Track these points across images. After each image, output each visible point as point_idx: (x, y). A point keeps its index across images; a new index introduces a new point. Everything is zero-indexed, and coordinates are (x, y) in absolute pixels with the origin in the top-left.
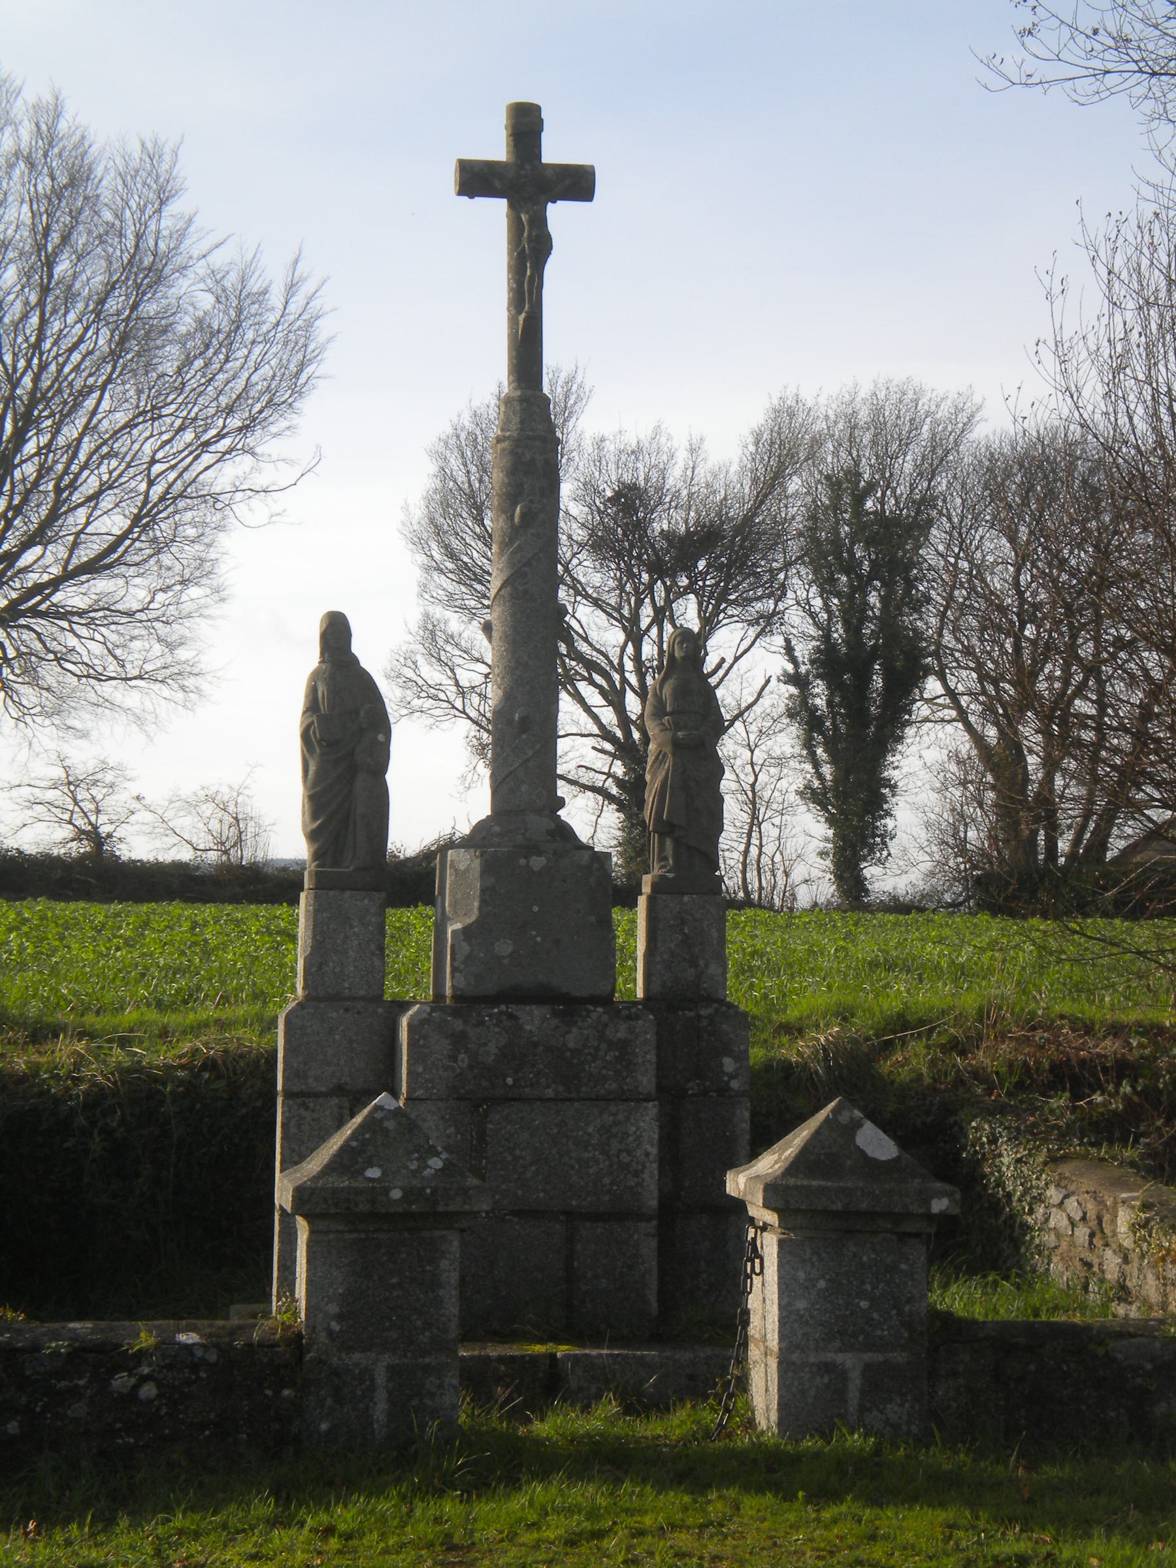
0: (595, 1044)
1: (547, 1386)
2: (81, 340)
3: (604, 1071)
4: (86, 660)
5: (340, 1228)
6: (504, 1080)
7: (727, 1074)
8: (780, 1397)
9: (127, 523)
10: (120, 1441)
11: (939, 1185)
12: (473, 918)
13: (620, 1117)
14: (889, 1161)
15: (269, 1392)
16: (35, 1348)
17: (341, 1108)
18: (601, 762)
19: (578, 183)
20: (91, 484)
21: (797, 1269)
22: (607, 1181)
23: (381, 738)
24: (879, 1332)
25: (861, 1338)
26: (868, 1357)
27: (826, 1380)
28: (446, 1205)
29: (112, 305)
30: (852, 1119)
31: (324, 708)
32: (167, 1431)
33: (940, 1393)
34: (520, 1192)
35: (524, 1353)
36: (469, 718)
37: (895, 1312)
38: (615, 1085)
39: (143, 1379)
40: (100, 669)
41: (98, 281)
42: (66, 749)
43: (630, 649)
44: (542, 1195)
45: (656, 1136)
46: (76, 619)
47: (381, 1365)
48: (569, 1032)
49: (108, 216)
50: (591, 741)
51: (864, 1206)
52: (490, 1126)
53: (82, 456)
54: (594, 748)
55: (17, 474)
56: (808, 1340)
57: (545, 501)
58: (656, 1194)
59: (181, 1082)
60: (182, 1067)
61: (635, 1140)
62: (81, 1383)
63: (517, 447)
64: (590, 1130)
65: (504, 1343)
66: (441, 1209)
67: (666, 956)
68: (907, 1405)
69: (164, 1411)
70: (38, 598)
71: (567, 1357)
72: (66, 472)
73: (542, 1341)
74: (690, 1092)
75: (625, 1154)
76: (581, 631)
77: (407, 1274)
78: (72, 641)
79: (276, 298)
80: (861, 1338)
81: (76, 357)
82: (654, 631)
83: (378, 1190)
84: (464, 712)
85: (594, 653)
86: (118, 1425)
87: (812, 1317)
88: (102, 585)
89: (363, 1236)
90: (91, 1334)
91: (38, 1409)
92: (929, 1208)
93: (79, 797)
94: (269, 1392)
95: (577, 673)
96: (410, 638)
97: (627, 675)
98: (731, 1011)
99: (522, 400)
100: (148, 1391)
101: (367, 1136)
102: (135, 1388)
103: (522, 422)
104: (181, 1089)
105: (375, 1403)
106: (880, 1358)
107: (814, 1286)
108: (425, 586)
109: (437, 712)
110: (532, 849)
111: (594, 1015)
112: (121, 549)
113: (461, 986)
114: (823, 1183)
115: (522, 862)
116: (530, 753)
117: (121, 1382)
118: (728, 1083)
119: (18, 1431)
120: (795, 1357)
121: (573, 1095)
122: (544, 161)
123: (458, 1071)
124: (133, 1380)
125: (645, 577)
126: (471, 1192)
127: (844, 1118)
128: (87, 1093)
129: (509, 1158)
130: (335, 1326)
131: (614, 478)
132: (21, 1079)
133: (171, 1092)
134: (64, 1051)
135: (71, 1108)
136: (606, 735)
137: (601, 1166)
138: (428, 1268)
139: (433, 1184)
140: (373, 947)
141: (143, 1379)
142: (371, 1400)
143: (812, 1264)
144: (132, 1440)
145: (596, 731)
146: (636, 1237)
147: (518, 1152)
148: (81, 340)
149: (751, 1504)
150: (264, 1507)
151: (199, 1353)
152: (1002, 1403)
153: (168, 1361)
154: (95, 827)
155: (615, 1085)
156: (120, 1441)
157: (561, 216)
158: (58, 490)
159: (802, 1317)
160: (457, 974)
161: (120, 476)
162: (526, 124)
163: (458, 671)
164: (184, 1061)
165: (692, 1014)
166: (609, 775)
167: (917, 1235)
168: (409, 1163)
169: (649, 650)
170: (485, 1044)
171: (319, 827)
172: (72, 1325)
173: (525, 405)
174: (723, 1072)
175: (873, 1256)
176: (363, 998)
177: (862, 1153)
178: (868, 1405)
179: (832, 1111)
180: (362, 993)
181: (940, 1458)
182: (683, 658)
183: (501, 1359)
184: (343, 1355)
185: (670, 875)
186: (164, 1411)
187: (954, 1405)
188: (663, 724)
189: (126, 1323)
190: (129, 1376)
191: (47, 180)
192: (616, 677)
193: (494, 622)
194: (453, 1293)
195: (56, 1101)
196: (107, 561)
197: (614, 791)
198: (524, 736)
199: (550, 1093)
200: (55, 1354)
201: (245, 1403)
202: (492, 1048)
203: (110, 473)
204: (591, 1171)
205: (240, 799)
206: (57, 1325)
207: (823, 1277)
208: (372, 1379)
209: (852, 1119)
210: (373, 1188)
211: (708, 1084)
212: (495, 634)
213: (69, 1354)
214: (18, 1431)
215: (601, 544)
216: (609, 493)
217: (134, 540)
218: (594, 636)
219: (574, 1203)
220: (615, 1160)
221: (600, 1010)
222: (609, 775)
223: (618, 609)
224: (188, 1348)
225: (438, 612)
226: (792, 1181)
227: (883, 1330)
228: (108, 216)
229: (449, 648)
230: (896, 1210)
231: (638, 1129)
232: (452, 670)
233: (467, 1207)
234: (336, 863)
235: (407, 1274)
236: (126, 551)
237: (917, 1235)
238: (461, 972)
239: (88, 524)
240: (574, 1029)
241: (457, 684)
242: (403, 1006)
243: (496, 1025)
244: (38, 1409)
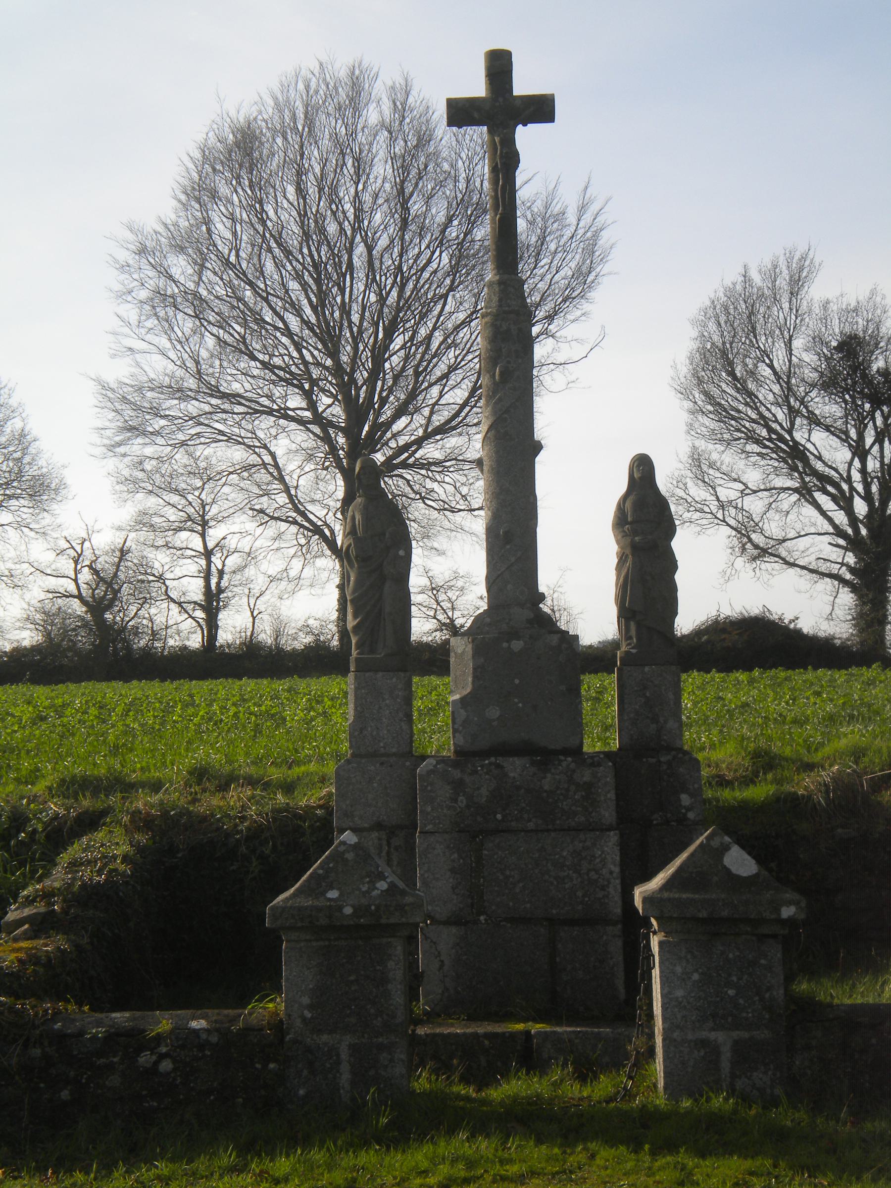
0: (566, 786)
1: (530, 1057)
2: (429, 261)
3: (573, 808)
4: (443, 497)
5: (308, 937)
6: (495, 816)
7: (685, 807)
8: (665, 1067)
9: (466, 394)
10: (147, 1105)
11: (788, 895)
12: (469, 690)
13: (588, 843)
14: (749, 877)
15: (258, 1066)
16: (81, 1033)
17: (380, 839)
18: (836, 554)
19: (541, 109)
20: (442, 368)
21: (675, 965)
22: (580, 894)
23: (401, 553)
24: (744, 1015)
25: (730, 1019)
26: (736, 1034)
27: (702, 1053)
28: (388, 919)
29: (453, 232)
30: (722, 844)
31: (360, 532)
32: (181, 1097)
33: (797, 1063)
34: (511, 904)
35: (505, 1030)
36: (728, 525)
37: (757, 998)
38: (583, 819)
39: (162, 1057)
40: (453, 504)
41: (441, 218)
42: (430, 564)
43: (857, 463)
44: (528, 905)
45: (618, 858)
46: (433, 468)
47: (344, 1044)
48: (545, 778)
49: (446, 166)
50: (827, 539)
51: (725, 913)
52: (485, 852)
53: (435, 345)
54: (830, 544)
55: (387, 365)
56: (686, 1021)
57: (520, 361)
58: (620, 903)
59: (319, 819)
60: (320, 807)
61: (601, 862)
62: (115, 1060)
63: (496, 320)
64: (565, 854)
65: (500, 1021)
66: (383, 921)
67: (632, 715)
68: (770, 1073)
69: (179, 1081)
70: (406, 455)
71: (539, 1033)
72: (421, 360)
73: (519, 1021)
74: (655, 822)
75: (593, 873)
76: (816, 452)
77: (362, 972)
78: (429, 484)
79: (571, 218)
80: (730, 1019)
81: (426, 275)
82: (876, 448)
83: (335, 908)
84: (724, 521)
85: (827, 469)
86: (144, 1093)
87: (689, 1003)
88: (452, 441)
89: (327, 943)
90: (126, 1022)
91: (84, 1081)
92: (779, 914)
93: (440, 599)
94: (258, 1066)
95: (815, 485)
96: (681, 466)
97: (855, 485)
98: (687, 757)
99: (500, 283)
100: (166, 1066)
101: (331, 865)
102: (156, 1063)
103: (500, 300)
104: (318, 824)
105: (341, 1074)
106: (745, 1035)
107: (690, 978)
108: (691, 425)
109: (704, 522)
110: (514, 635)
111: (564, 764)
112: (463, 414)
113: (461, 744)
114: (691, 896)
115: (505, 645)
116: (513, 559)
117: (145, 1059)
118: (685, 815)
119: (69, 1098)
120: (675, 1035)
121: (550, 827)
122: (515, 94)
123: (459, 810)
124: (154, 1058)
125: (867, 406)
126: (406, 908)
127: (716, 843)
128: (248, 829)
129: (501, 877)
130: (308, 1014)
131: (837, 331)
132: (204, 819)
133: (309, 826)
134: (235, 797)
135: (238, 840)
136: (839, 532)
137: (575, 882)
138: (378, 968)
139: (377, 902)
140: (401, 715)
141: (162, 1057)
142: (338, 1071)
143: (687, 960)
144: (155, 1104)
145: (831, 530)
146: (605, 938)
147: (508, 873)
148: (429, 261)
149: (605, 1154)
150: (229, 1157)
151: (204, 1036)
152: (849, 1070)
153: (180, 1042)
154: (452, 621)
155: (583, 819)
156: (147, 1105)
157: (527, 137)
158: (417, 374)
159: (680, 1003)
160: (457, 735)
161: (462, 360)
162: (499, 65)
163: (718, 489)
164: (321, 802)
165: (654, 760)
166: (842, 564)
167: (774, 936)
168: (361, 886)
169: (872, 465)
170: (478, 789)
171: (358, 623)
172: (114, 1015)
173: (502, 286)
174: (681, 805)
175: (738, 953)
176: (394, 754)
177: (728, 871)
178: (738, 1073)
179: (706, 838)
180: (394, 750)
181: (788, 1117)
182: (640, 478)
183: (487, 1035)
184: (315, 1037)
185: (634, 651)
186: (179, 1081)
187: (809, 1072)
188: (624, 531)
189: (150, 1013)
190: (151, 1054)
191: (402, 143)
192: (845, 487)
193: (485, 459)
194: (399, 987)
195: (228, 835)
196: (454, 423)
197: (848, 576)
198: (508, 547)
199: (531, 825)
200: (94, 1037)
201: (240, 1074)
202: (484, 791)
203: (456, 358)
204: (567, 886)
205: (555, 596)
206: (103, 1015)
207: (696, 971)
208: (338, 1055)
209: (722, 844)
210: (330, 906)
211: (669, 815)
212: (485, 468)
213: (105, 1038)
214: (69, 1098)
215: (829, 384)
216: (834, 344)
217: (472, 407)
218: (826, 456)
219: (554, 912)
220: (586, 877)
221: (569, 759)
222: (842, 564)
223: (846, 433)
224: (196, 1032)
225: (702, 444)
226: (666, 895)
227: (748, 1013)
228: (446, 166)
229: (711, 471)
230: (752, 917)
231: (603, 852)
232: (714, 488)
233: (404, 920)
234: (372, 651)
235: (362, 972)
236: (467, 415)
237: (774, 936)
238: (460, 733)
239: (441, 396)
240: (549, 775)
241: (718, 499)
242: (423, 758)
243: (487, 773)
244: (84, 1081)
